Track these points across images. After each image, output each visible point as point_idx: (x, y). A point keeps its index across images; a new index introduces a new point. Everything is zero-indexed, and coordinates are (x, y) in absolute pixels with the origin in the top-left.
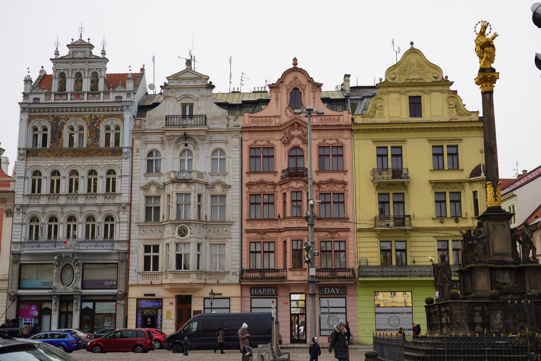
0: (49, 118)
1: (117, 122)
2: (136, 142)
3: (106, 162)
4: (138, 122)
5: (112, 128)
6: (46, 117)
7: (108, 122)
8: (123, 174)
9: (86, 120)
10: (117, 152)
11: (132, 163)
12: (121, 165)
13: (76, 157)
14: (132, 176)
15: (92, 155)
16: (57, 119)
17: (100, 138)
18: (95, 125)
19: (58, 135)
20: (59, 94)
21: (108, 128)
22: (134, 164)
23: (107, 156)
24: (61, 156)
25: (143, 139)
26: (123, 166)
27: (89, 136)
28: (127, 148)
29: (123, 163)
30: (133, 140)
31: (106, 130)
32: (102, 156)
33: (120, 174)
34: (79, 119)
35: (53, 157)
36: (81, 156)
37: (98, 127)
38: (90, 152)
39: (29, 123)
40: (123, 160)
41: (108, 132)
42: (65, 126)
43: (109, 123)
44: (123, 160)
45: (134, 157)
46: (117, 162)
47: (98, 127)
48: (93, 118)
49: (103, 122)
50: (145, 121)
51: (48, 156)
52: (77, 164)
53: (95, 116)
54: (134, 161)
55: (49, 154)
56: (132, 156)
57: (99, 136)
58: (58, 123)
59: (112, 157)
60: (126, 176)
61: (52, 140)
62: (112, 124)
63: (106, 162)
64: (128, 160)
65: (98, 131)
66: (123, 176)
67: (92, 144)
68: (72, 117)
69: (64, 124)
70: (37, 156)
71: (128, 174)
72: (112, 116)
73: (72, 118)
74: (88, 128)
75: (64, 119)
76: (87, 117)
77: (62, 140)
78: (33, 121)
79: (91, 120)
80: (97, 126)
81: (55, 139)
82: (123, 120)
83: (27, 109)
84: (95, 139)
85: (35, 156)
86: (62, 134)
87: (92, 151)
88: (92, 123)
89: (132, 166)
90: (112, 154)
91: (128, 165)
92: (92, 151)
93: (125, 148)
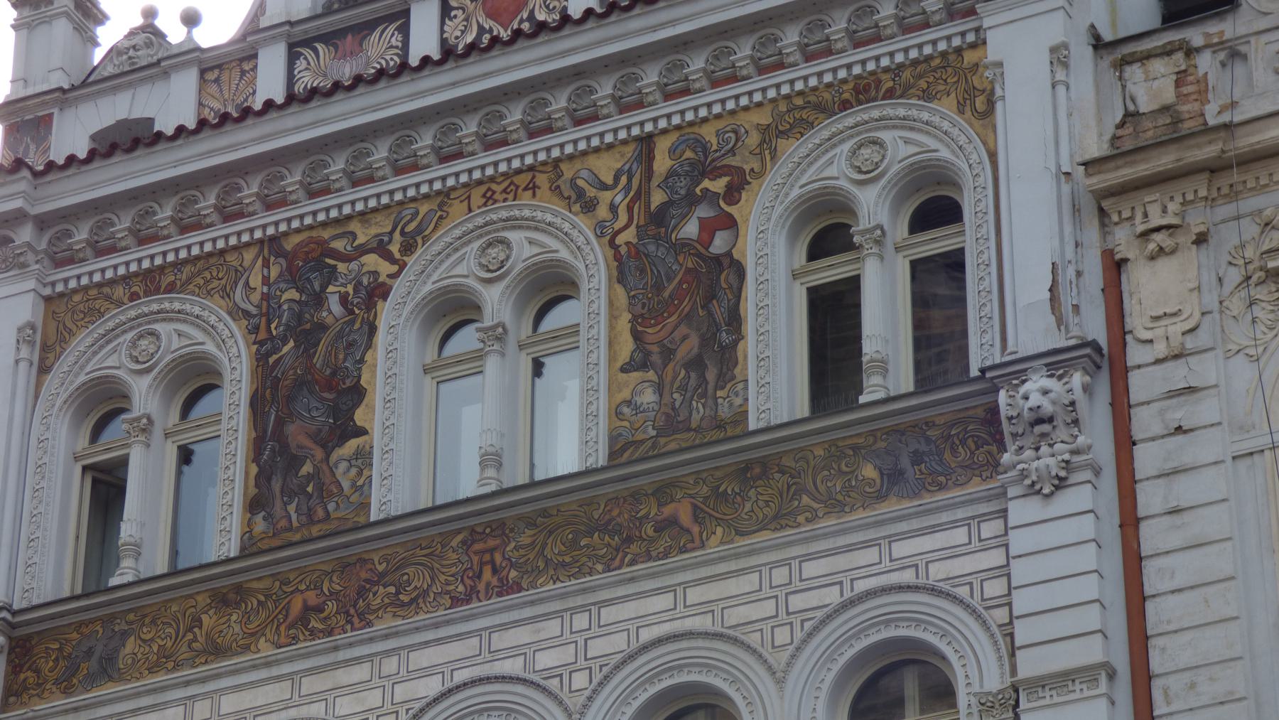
0: (239, 273)
1: (915, 135)
2: (1156, 287)
3: (830, 580)
4: (1152, 86)
5: (874, 207)
6: (209, 273)
7: (821, 161)
8: (1029, 665)
9: (589, 207)
10: (956, 434)
11: (1130, 522)
12: (1004, 571)
13: (506, 588)
14: (1142, 678)
15: (673, 539)
16: (308, 262)
17: (750, 346)
18: (691, 229)
19: (321, 418)
20: (329, 38)
21: (829, 233)
22: (1152, 536)
23: (836, 506)
24: (355, 612)
25: (1228, 237)
26: (1021, 572)
27: (627, 346)
28: (1056, 362)
29: (1019, 542)
30: (1115, 267)
31: (817, 250)
32: (779, 520)
33: (994, 681)
34: (526, 206)
35: (265, 649)
36: (559, 569)
37: (719, 243)
38: (650, 508)
39: (44, 369)
40: (1020, 510)
41: (832, 271)
42: (386, 313)
43: (835, 169)
44: (1020, 510)
45: (1146, 459)
46: (952, 553)
47: (719, 243)
48: (662, 163)
49: (776, 174)
50: (1234, 53)
51: (216, 651)
52: (512, 666)
53: (686, 132)
54: (1149, 498)
55: (234, 624)
56: (1125, 443)
57: (735, 320)
58: (319, 300)
59: (892, 507)
60: (1063, 679)
61: (263, 478)
62: (867, 176)
63: (830, 580)
64: (1076, 498)
65: (718, 279)
66: (1040, 683)
67: (672, 423)
68: (457, 208)
69: (378, 291)
70: (108, 670)
71: (1090, 652)
72: (864, 90)
73: (458, 221)
74: (621, 277)
75: (381, 249)
76: (606, 167)
77: (363, 458)
78: (82, 341)
79: (642, 195)
80: (709, 229)
81: (294, 462)
82: (980, 103)
83: (25, 234)
84: (696, 364)
85: (92, 681)
86: (358, 393)
87: (663, 493)
88: (659, 219)
89: (1133, 562)
90: (893, 480)
91: (1087, 558)
92: (663, 493)
93: (1015, 371)
